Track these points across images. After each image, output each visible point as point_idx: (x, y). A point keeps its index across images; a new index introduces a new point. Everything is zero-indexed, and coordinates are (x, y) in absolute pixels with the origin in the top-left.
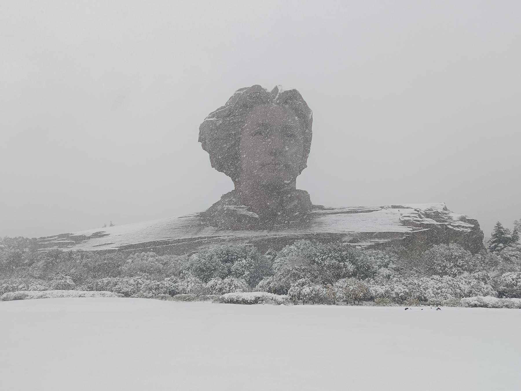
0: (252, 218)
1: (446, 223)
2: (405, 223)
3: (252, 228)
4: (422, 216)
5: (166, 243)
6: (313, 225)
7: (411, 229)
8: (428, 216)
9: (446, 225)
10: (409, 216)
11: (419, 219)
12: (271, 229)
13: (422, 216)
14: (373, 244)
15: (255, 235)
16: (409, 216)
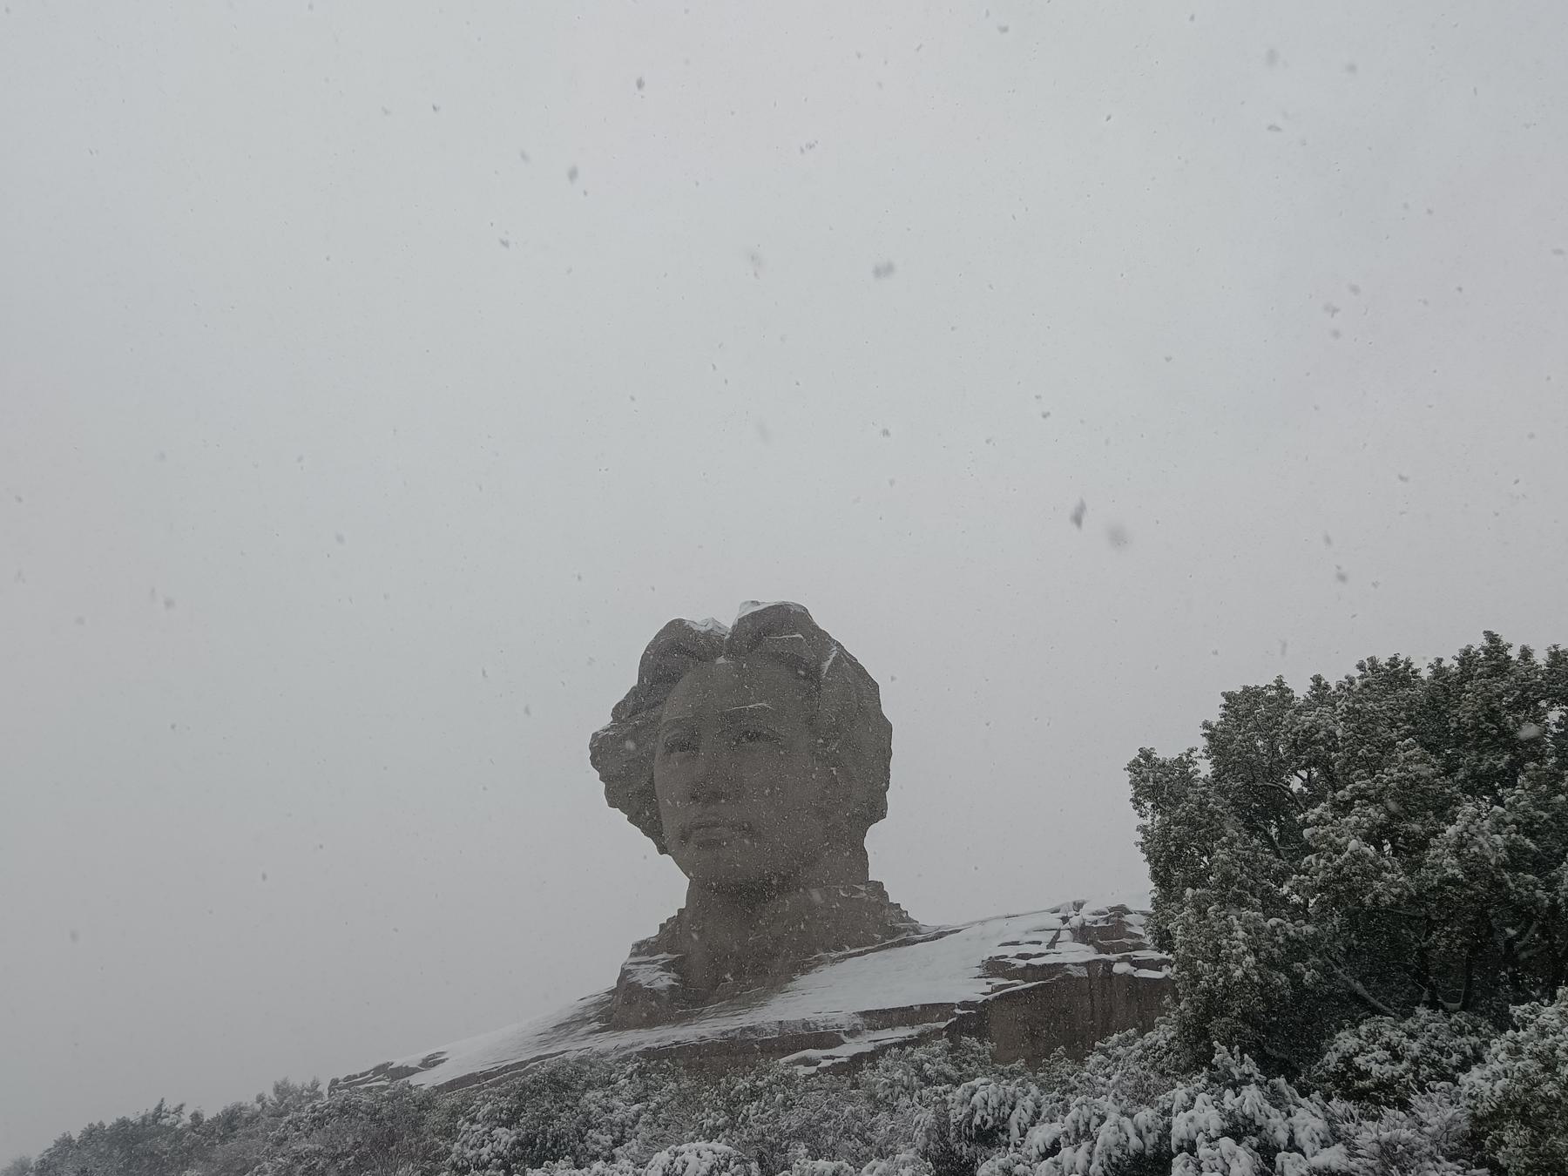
0: (654, 994)
1: (1112, 957)
2: (994, 967)
3: (651, 1022)
4: (1065, 935)
5: (487, 1075)
6: (780, 996)
7: (988, 989)
8: (1083, 934)
9: (1109, 964)
10: (1016, 943)
11: (1042, 949)
12: (680, 1020)
13: (1065, 935)
14: (869, 1048)
15: (623, 1043)
16: (1016, 943)
